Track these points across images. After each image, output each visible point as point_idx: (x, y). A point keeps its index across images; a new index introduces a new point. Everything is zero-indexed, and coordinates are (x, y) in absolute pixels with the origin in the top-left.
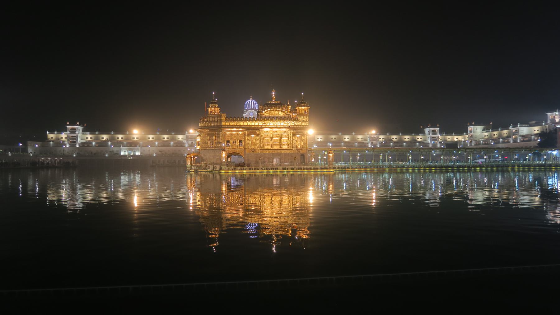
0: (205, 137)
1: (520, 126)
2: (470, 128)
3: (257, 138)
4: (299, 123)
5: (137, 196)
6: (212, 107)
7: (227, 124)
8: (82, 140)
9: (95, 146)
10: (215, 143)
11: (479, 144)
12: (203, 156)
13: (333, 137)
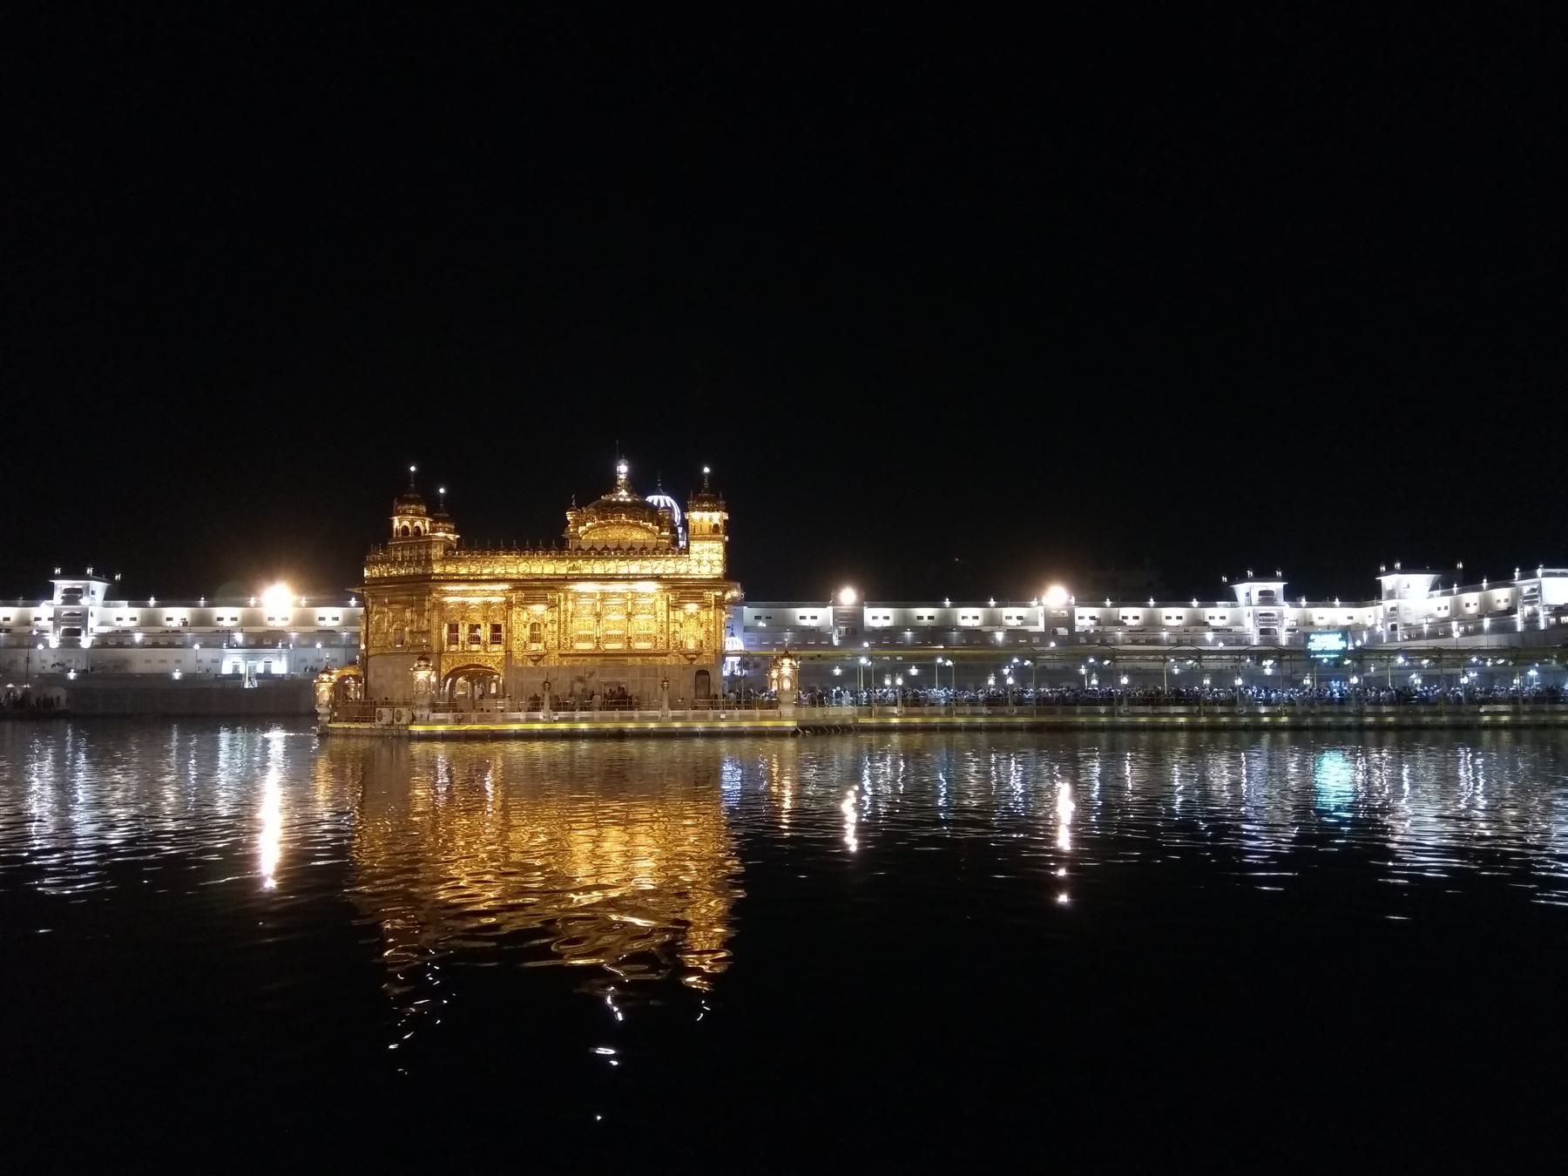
1: (1545, 575)
5: (269, 808)
7: (450, 569)
8: (102, 624)
9: (143, 646)
11: (1419, 636)
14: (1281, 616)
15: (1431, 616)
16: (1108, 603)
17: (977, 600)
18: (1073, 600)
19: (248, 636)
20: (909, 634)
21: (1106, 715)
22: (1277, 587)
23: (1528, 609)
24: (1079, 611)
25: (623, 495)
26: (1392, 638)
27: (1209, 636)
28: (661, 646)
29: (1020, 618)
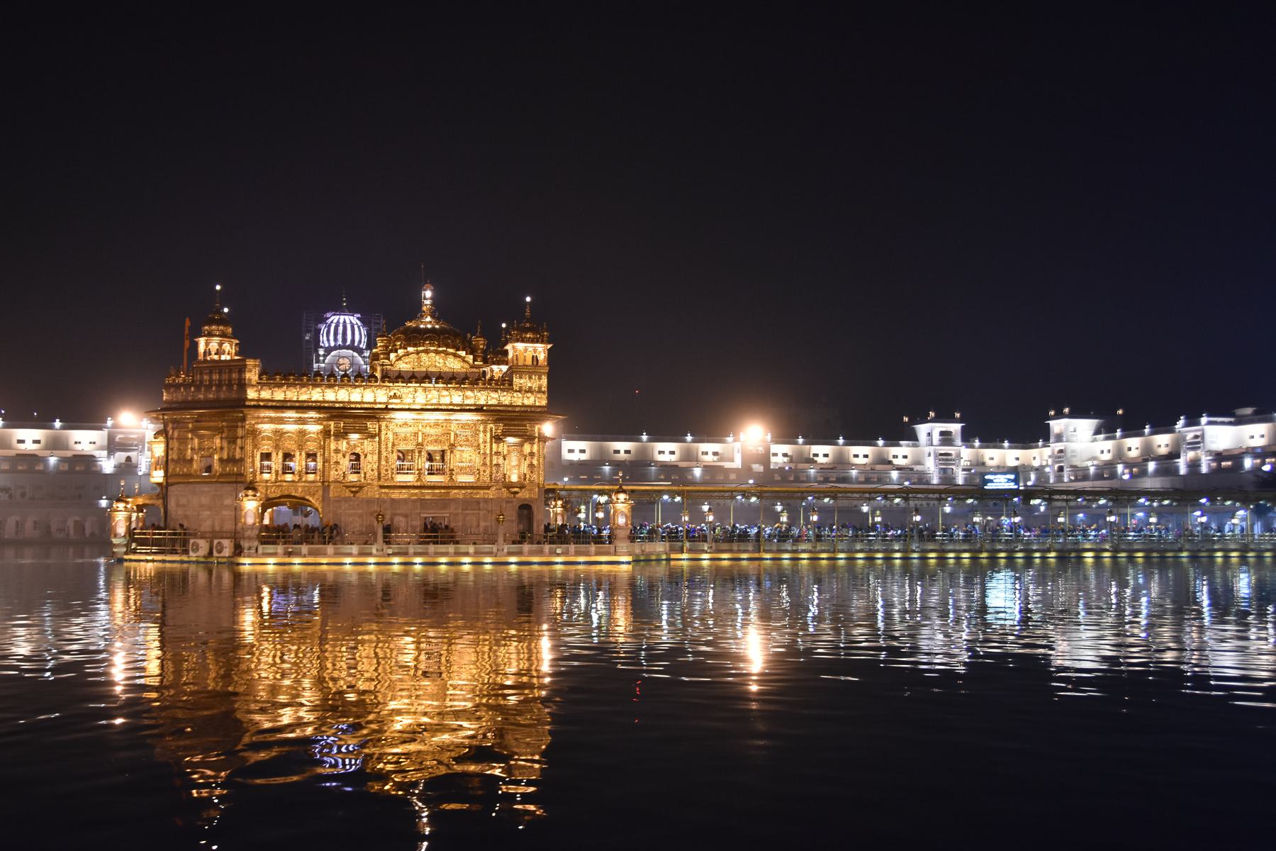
2: (1056, 425)
3: (368, 446)
4: (518, 400)
7: (266, 394)
10: (221, 460)
11: (1085, 478)
13: (622, 446)
14: (959, 456)
15: (1094, 458)
16: (801, 440)
17: (676, 437)
18: (769, 437)
20: (607, 469)
23: (1191, 454)
24: (775, 448)
25: (427, 322)
26: (1059, 478)
27: (895, 475)
28: (485, 478)
29: (715, 454)
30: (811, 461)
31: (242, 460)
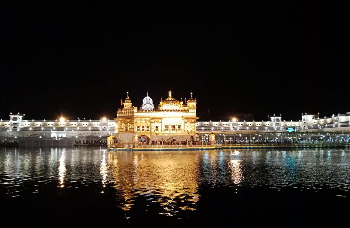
0: (121, 124)
1: (340, 116)
2: (303, 117)
6: (126, 102)
8: (21, 126)
10: (129, 128)
12: (120, 137)
13: (206, 123)
14: (281, 124)
15: (312, 124)
19: (57, 128)
21: (273, 145)
22: (280, 118)
23: (336, 123)
25: (170, 99)
26: (304, 129)
27: (266, 128)
30: (247, 126)
31: (134, 128)
